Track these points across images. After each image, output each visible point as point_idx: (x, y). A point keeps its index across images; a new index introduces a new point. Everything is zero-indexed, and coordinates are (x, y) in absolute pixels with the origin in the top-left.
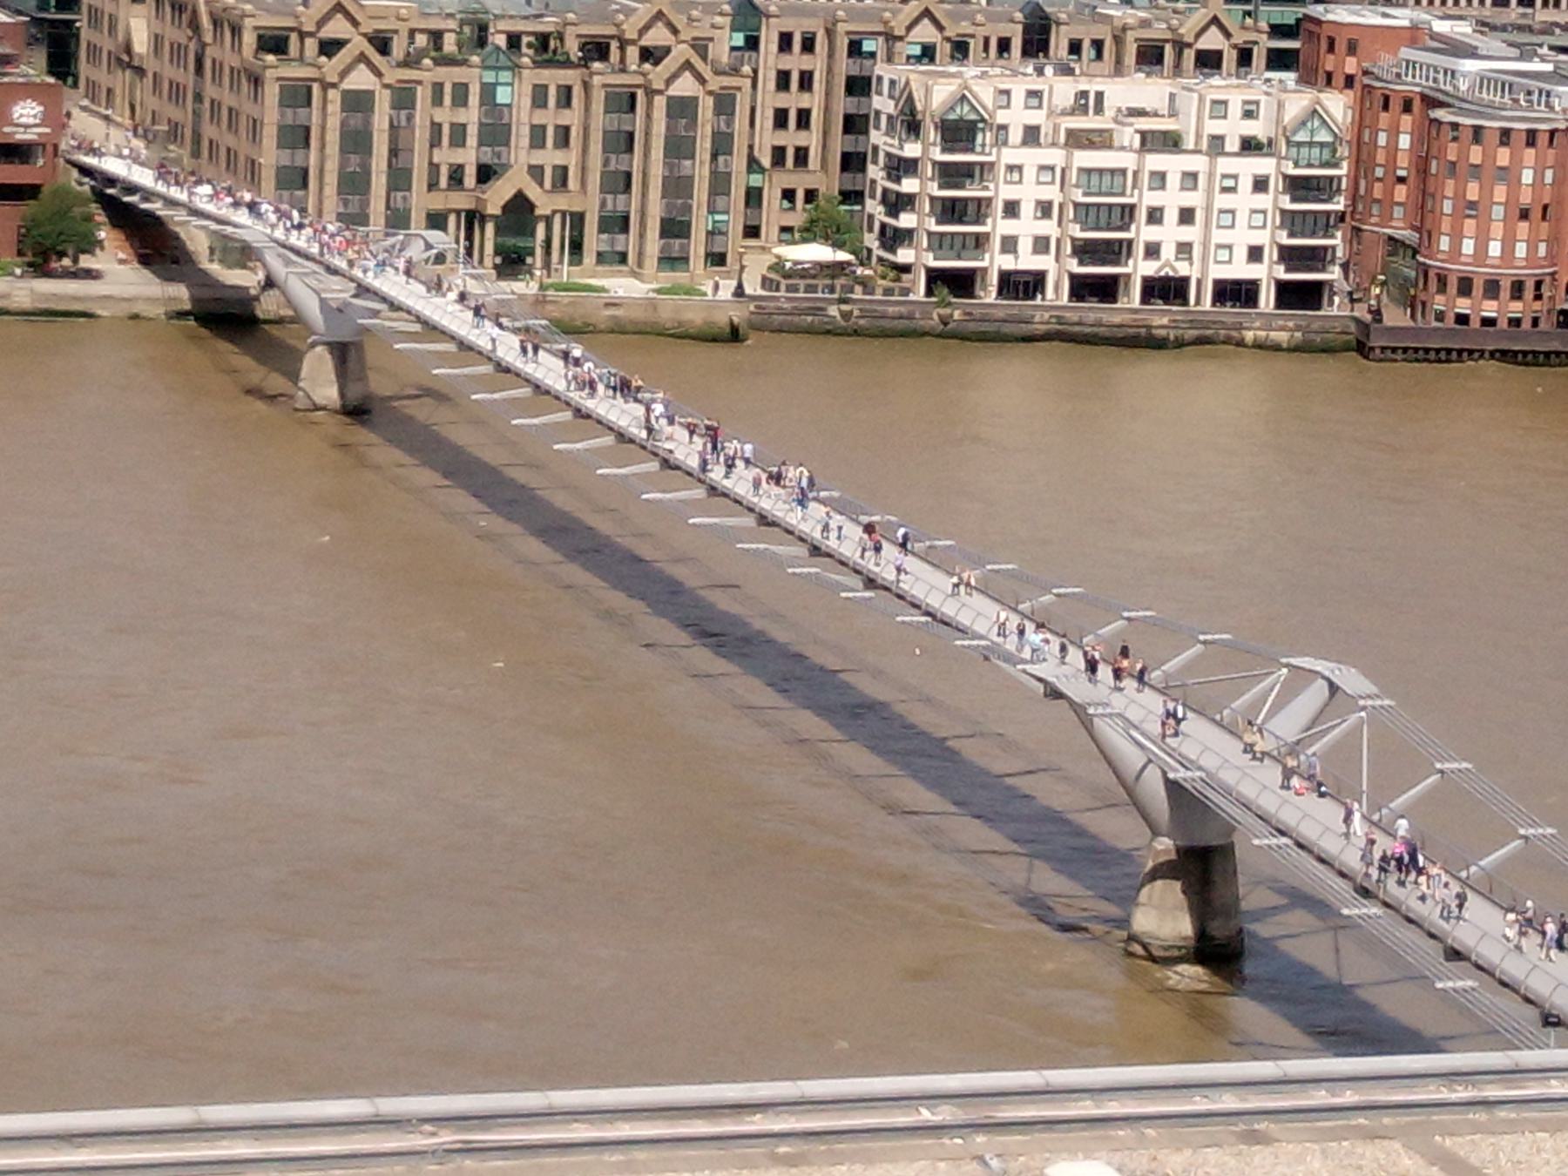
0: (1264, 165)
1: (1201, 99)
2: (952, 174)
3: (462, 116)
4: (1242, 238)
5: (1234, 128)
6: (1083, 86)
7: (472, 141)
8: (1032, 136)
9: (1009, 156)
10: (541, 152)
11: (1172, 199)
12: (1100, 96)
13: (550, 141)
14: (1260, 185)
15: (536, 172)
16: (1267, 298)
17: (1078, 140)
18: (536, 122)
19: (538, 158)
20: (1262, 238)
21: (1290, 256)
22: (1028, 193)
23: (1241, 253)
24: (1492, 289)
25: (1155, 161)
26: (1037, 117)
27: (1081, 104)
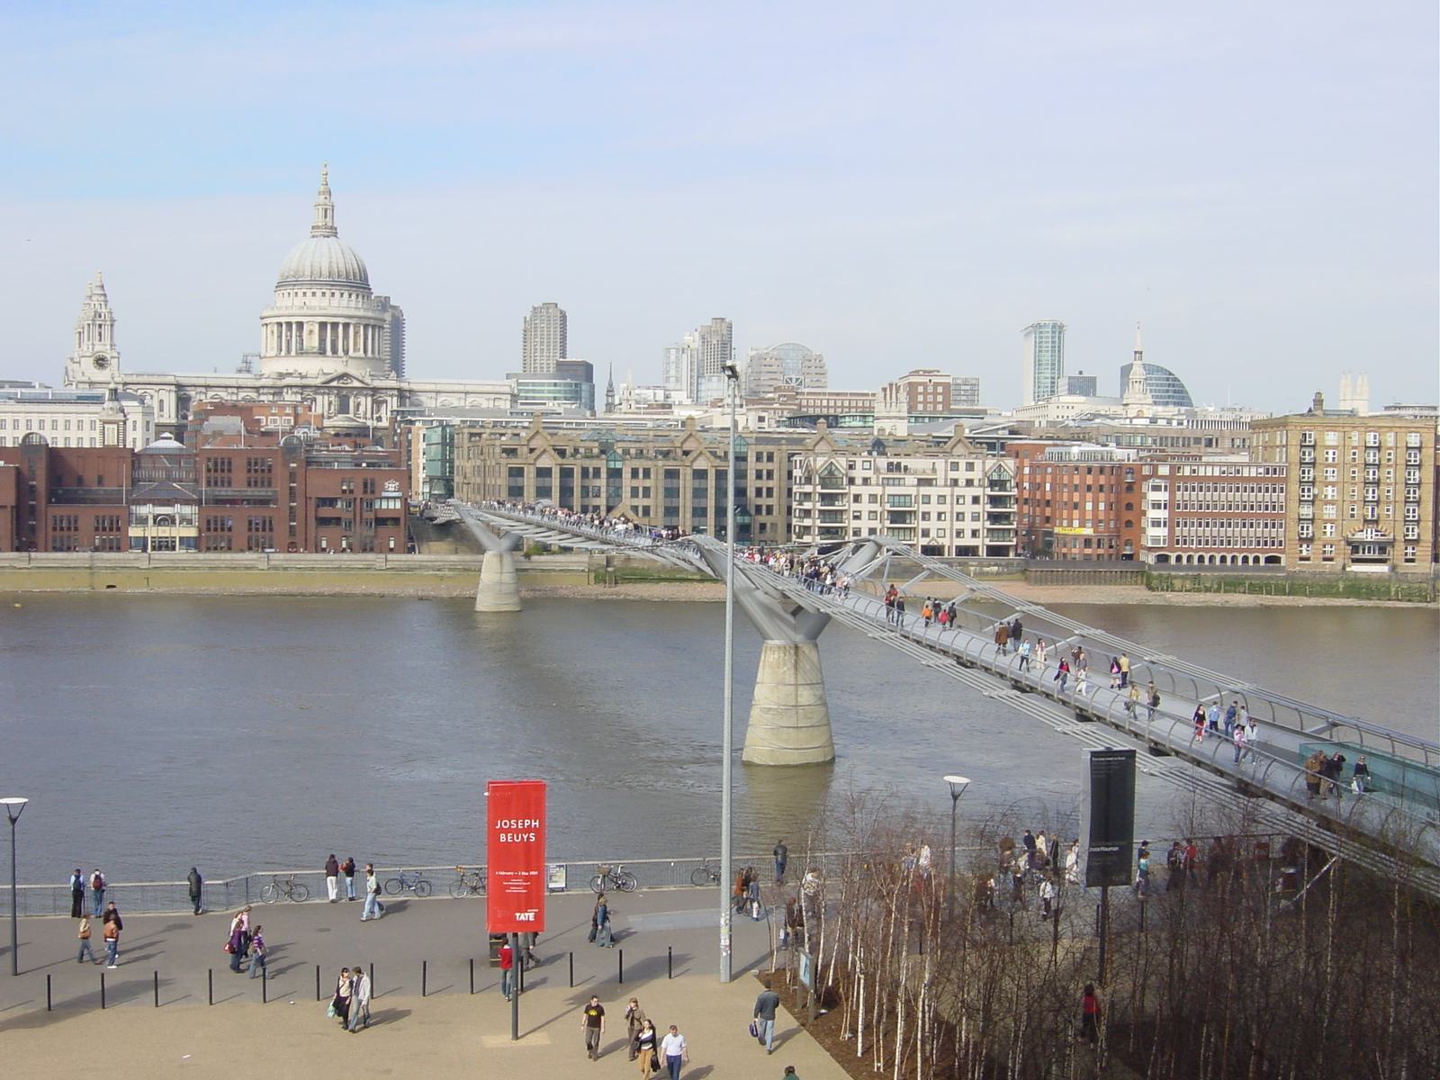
1: (946, 462)
3: (597, 482)
4: (968, 525)
5: (962, 475)
6: (891, 460)
7: (603, 495)
8: (866, 481)
9: (854, 490)
10: (636, 499)
12: (899, 464)
13: (641, 494)
14: (976, 500)
15: (635, 509)
16: (982, 552)
17: (886, 482)
18: (633, 485)
19: (635, 502)
20: (977, 525)
23: (968, 533)
25: (925, 490)
26: (869, 474)
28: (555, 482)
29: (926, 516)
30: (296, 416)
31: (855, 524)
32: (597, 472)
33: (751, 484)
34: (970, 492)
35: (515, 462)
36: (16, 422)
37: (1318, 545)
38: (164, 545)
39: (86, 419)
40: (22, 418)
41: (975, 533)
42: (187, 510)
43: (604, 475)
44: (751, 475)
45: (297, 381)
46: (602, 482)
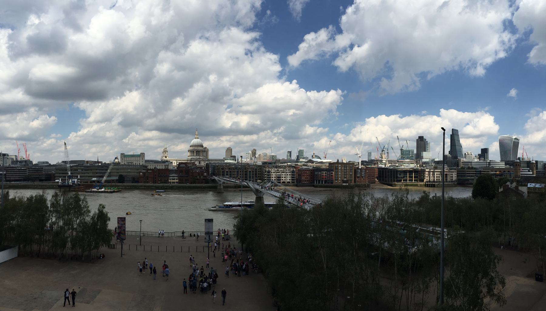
0: (290, 174)
2: (268, 175)
4: (289, 178)
7: (236, 175)
8: (274, 172)
9: (272, 174)
11: (284, 176)
14: (290, 175)
16: (291, 183)
17: (277, 172)
20: (290, 179)
21: (292, 180)
22: (274, 176)
23: (289, 180)
24: (306, 181)
25: (282, 174)
26: (274, 171)
27: (277, 170)
28: (229, 173)
29: (283, 177)
30: (193, 164)
31: (272, 179)
32: (235, 172)
33: (258, 173)
34: (289, 174)
35: (223, 170)
36: (154, 165)
37: (338, 181)
38: (174, 183)
39: (164, 165)
40: (155, 165)
41: (290, 180)
42: (177, 178)
43: (236, 172)
44: (258, 172)
45: (193, 159)
46: (236, 173)
